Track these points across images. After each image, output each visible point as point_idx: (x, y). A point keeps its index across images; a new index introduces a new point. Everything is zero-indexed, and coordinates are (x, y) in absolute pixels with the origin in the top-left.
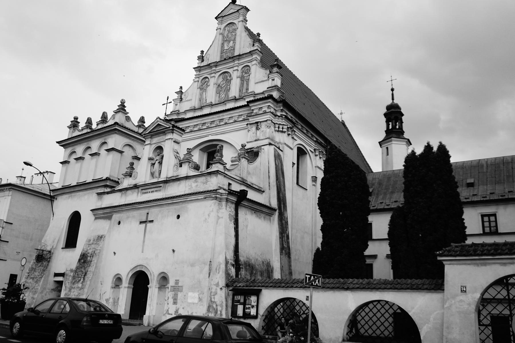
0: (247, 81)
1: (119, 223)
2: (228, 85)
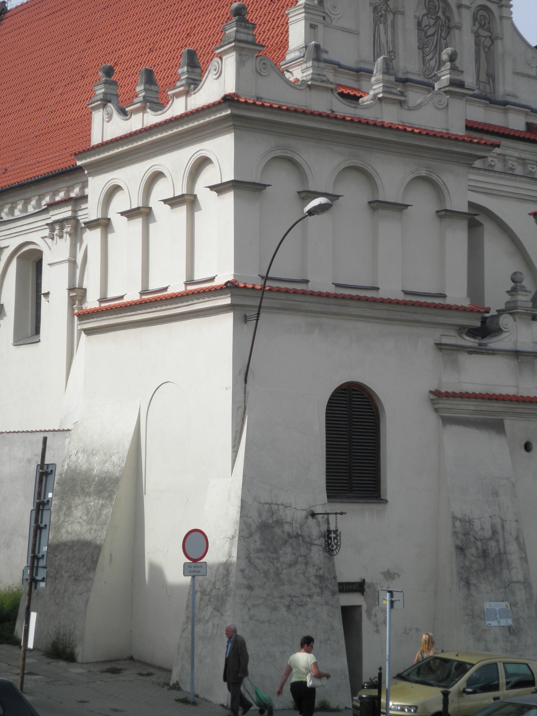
0: (486, 50)
1: (528, 447)
2: (441, 36)
